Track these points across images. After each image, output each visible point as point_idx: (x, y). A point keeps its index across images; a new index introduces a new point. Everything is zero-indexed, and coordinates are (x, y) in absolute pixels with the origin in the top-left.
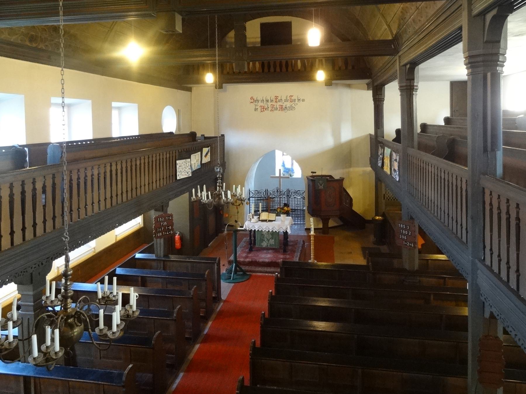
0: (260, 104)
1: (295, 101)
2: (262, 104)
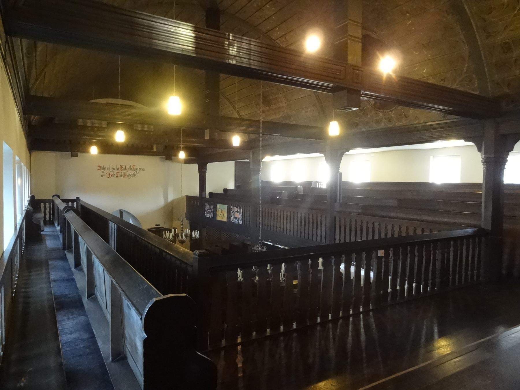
0: (107, 171)
2: (108, 171)
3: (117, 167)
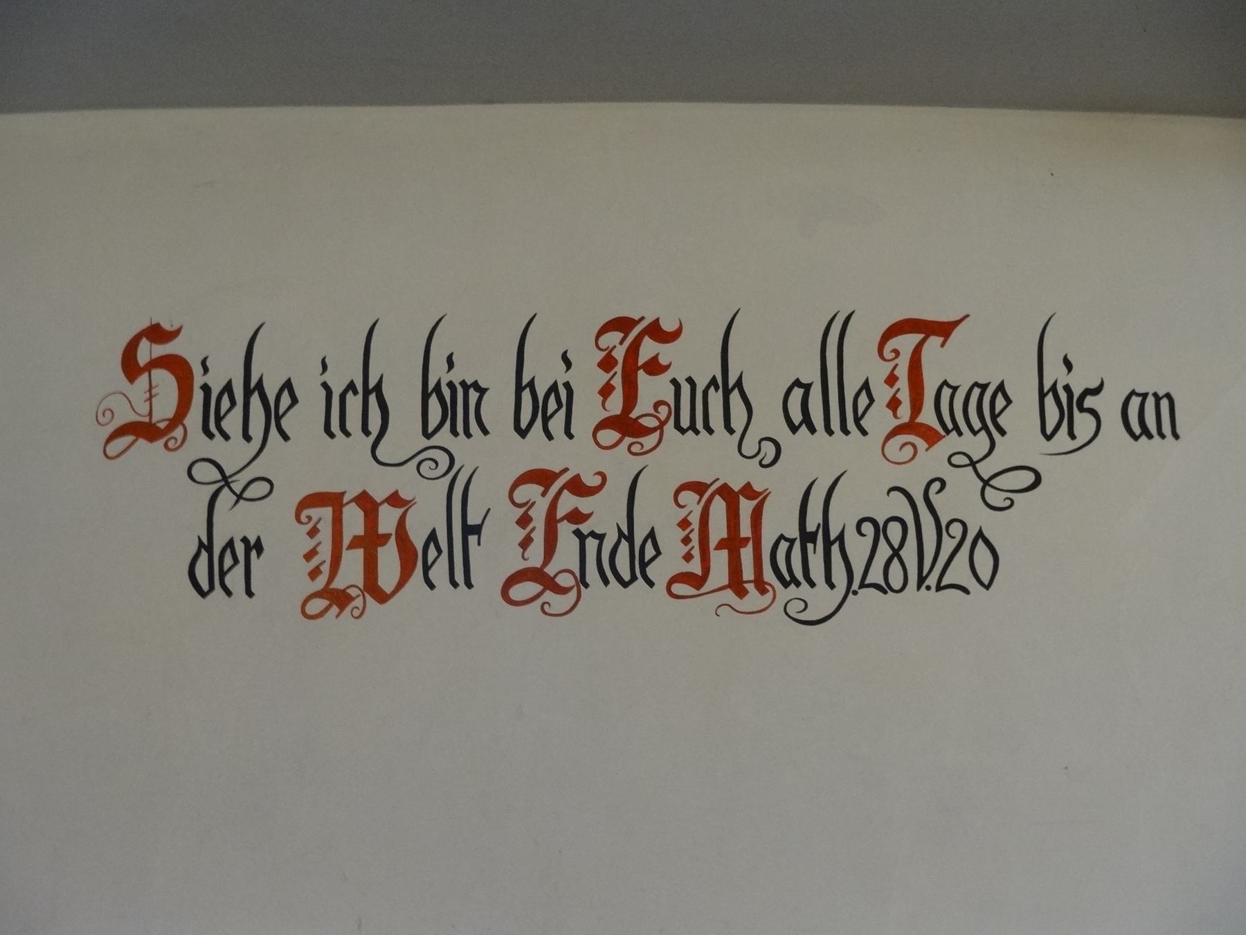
1: (992, 426)
3: (544, 371)
